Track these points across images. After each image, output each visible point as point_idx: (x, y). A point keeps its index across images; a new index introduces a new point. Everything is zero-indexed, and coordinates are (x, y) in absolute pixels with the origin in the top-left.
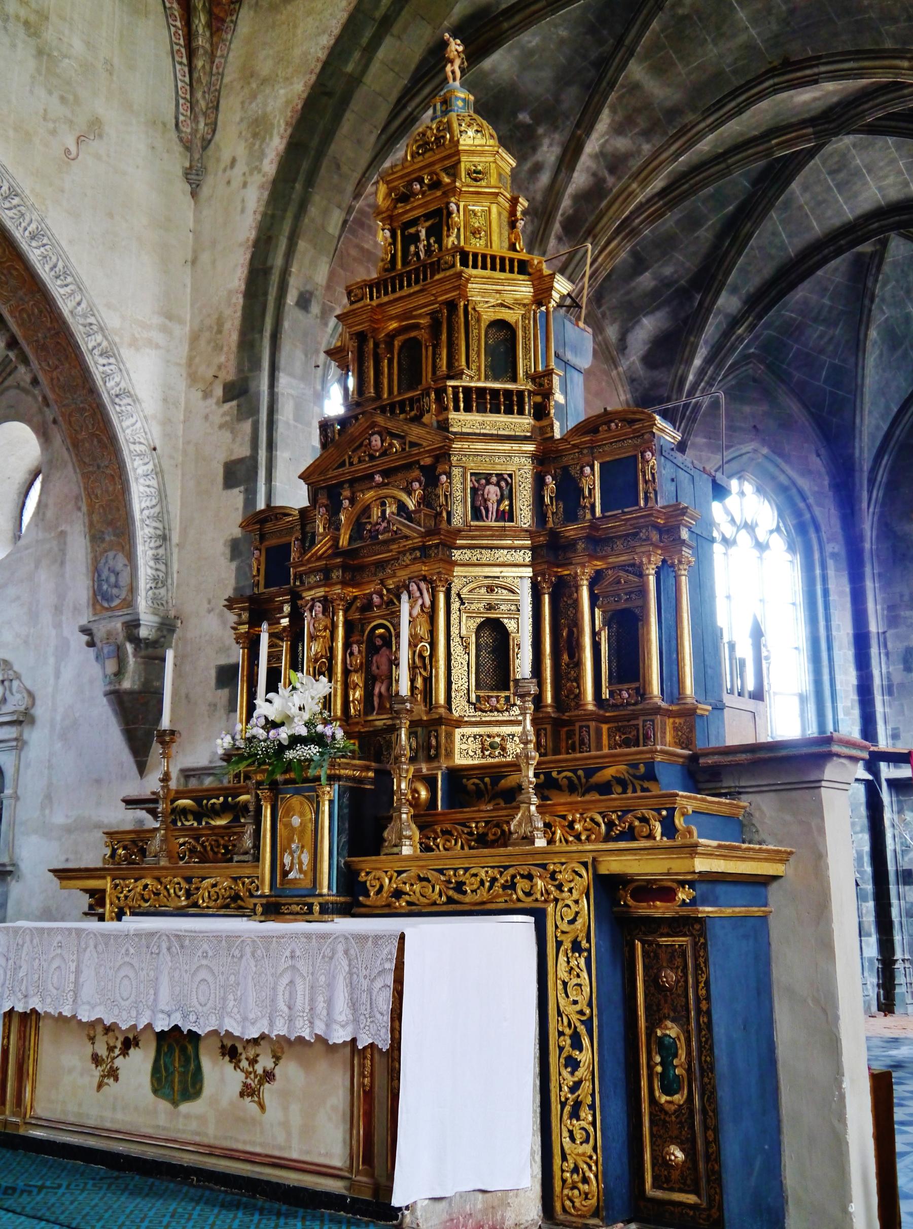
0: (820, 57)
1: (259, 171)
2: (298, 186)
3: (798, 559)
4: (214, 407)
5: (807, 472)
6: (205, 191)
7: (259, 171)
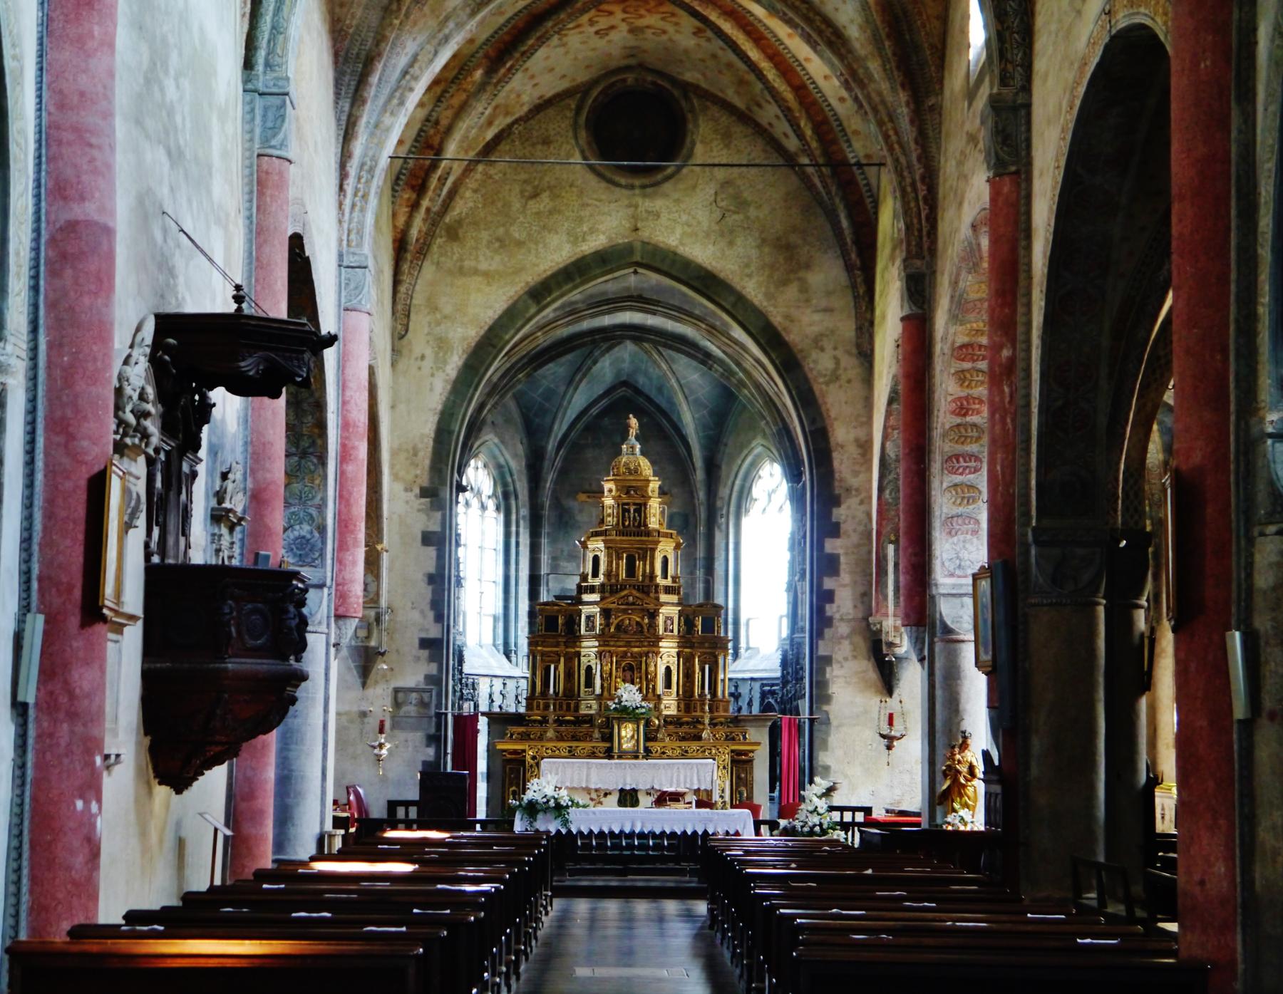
0: (659, 302)
1: (444, 371)
2: (471, 391)
3: (501, 517)
4: (413, 498)
5: (515, 456)
6: (401, 366)
7: (444, 371)
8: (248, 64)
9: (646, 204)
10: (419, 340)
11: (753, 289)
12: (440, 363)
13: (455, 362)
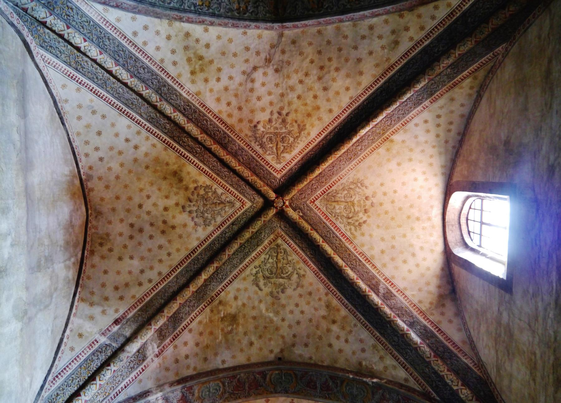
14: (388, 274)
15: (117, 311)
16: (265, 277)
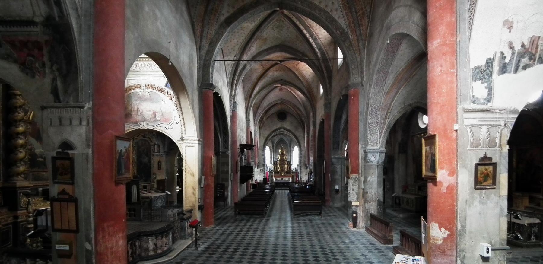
8: (246, 118)
9: (283, 123)
10: (261, 136)
11: (293, 131)
12: (264, 138)
13: (265, 139)
14: (316, 32)
15: (234, 54)
16: (276, 28)
